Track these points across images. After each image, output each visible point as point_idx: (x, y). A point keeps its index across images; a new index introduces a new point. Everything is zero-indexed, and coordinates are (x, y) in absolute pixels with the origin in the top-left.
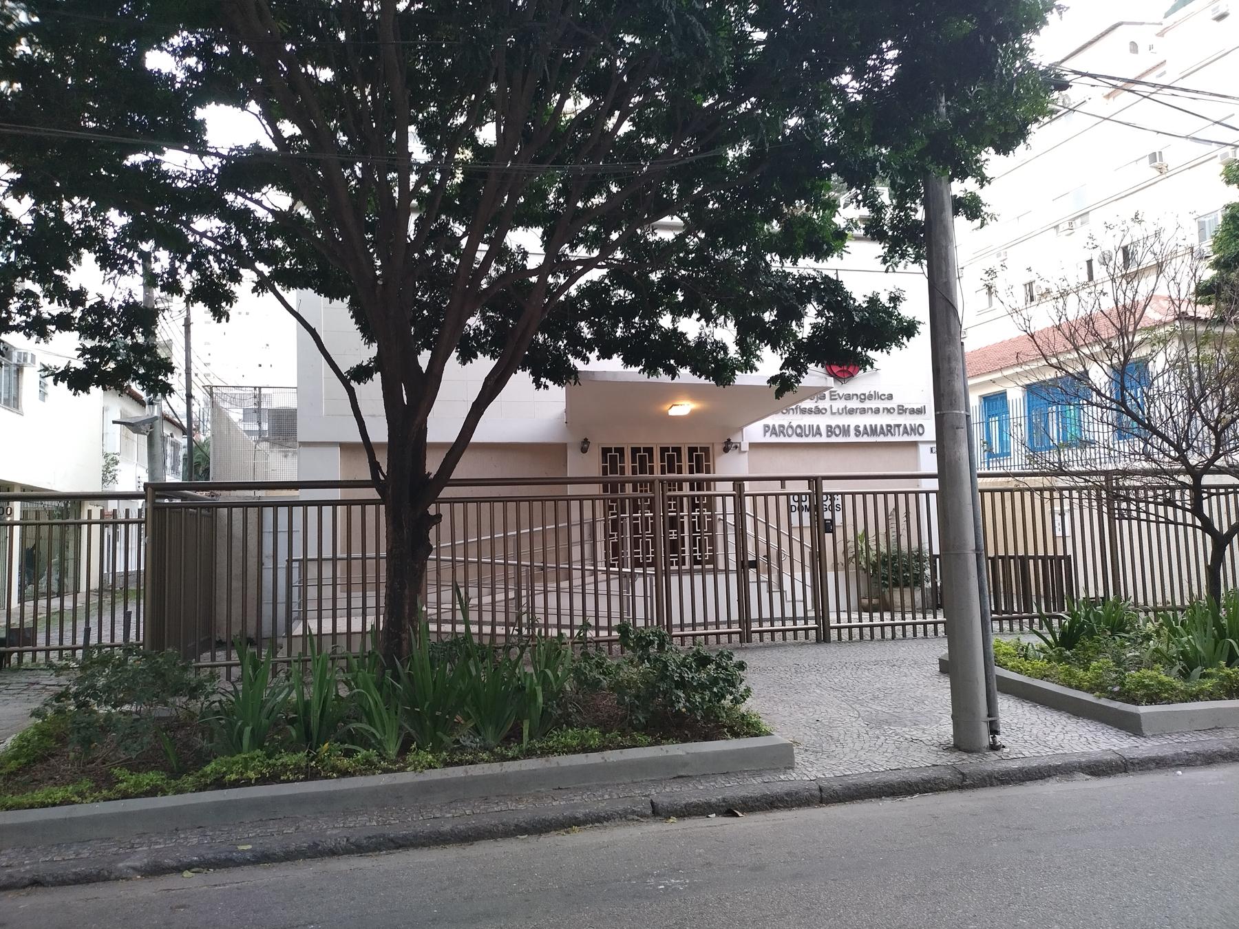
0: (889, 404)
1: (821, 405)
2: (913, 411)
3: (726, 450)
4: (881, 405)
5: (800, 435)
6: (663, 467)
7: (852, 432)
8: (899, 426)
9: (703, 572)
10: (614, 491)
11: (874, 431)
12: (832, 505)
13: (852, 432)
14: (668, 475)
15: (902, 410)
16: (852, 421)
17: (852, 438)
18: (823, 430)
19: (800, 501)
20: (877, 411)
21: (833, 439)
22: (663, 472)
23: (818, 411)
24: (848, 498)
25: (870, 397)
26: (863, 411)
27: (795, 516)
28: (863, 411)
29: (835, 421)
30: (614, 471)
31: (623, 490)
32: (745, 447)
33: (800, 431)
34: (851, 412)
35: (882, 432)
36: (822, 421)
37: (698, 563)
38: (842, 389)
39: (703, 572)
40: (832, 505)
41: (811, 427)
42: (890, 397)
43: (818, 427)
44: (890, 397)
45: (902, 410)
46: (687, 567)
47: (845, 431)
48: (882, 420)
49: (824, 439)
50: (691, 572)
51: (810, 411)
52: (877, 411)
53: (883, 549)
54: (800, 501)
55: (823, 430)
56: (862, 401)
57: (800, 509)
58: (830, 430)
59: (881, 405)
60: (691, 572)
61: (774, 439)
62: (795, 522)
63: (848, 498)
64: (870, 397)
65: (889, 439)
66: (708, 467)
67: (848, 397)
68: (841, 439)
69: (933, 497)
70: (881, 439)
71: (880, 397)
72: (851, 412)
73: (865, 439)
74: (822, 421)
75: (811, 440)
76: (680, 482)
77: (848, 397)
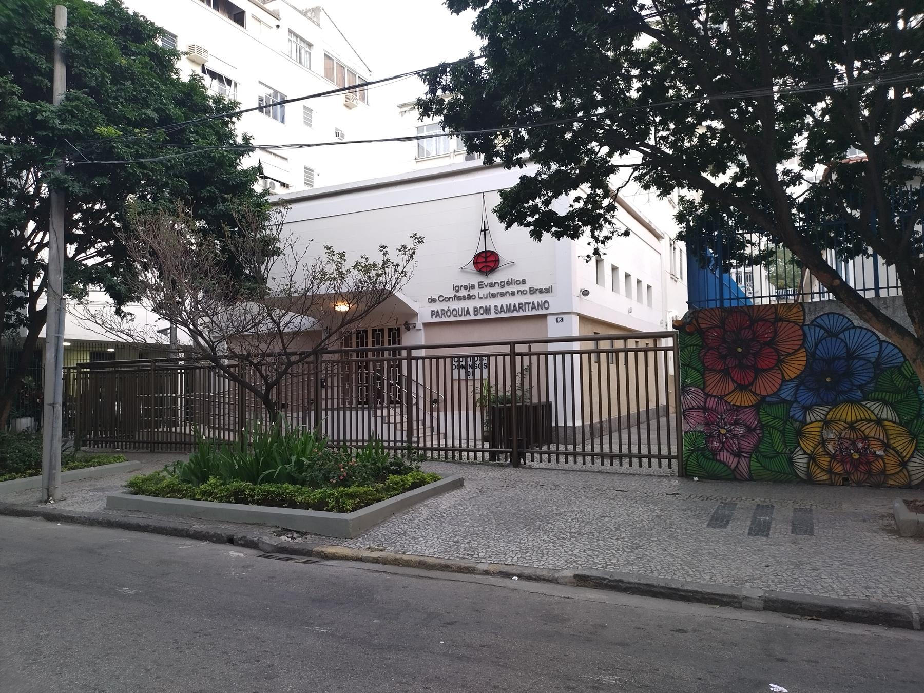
0: (522, 287)
1: (472, 292)
2: (541, 291)
3: (409, 329)
4: (515, 288)
5: (455, 316)
6: (389, 341)
7: (493, 310)
8: (529, 303)
9: (363, 409)
10: (394, 355)
11: (508, 309)
12: (481, 364)
13: (493, 310)
14: (376, 347)
15: (533, 291)
16: (491, 303)
17: (493, 315)
18: (472, 311)
19: (459, 362)
20: (513, 293)
21: (479, 317)
22: (389, 344)
23: (470, 297)
24: (492, 359)
25: (508, 283)
26: (502, 294)
27: (456, 371)
28: (502, 294)
29: (477, 303)
30: (378, 344)
31: (399, 355)
32: (420, 325)
33: (456, 312)
34: (494, 296)
35: (515, 309)
36: (470, 305)
37: (360, 403)
38: (486, 281)
39: (363, 409)
40: (481, 364)
41: (463, 309)
42: (524, 282)
43: (468, 309)
44: (524, 282)
45: (533, 291)
46: (354, 405)
47: (488, 310)
48: (523, 299)
49: (472, 317)
50: (357, 409)
51: (464, 298)
52: (513, 293)
53: (501, 394)
54: (459, 362)
55: (472, 311)
56: (503, 287)
57: (459, 367)
58: (476, 311)
59: (515, 288)
60: (357, 409)
61: (438, 320)
62: (456, 377)
63: (492, 359)
64: (508, 283)
65: (521, 314)
66: (399, 341)
67: (491, 285)
68: (485, 317)
69: (671, 354)
70: (515, 314)
71: (517, 282)
72: (494, 296)
73: (503, 315)
74: (470, 305)
75: (463, 318)
76: (367, 351)
77: (491, 285)
